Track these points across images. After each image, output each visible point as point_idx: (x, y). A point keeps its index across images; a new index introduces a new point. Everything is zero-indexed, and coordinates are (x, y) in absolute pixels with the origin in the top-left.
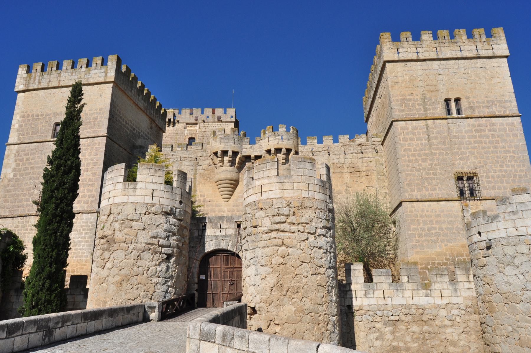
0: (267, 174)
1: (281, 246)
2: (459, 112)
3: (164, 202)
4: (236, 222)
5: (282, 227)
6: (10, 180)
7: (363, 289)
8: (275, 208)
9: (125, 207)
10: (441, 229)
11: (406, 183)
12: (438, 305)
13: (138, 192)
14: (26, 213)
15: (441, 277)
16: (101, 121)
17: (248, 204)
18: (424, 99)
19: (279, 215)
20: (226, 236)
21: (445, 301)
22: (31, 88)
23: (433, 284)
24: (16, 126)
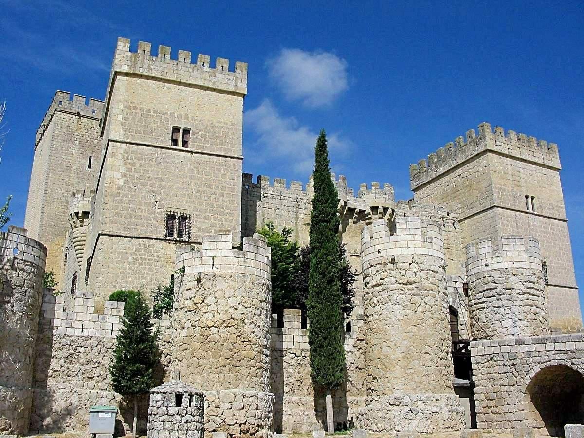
0: (517, 247)
5: (532, 291)
6: (120, 188)
13: (435, 247)
14: (148, 235)
16: (232, 139)
18: (513, 191)
22: (137, 72)
24: (120, 118)
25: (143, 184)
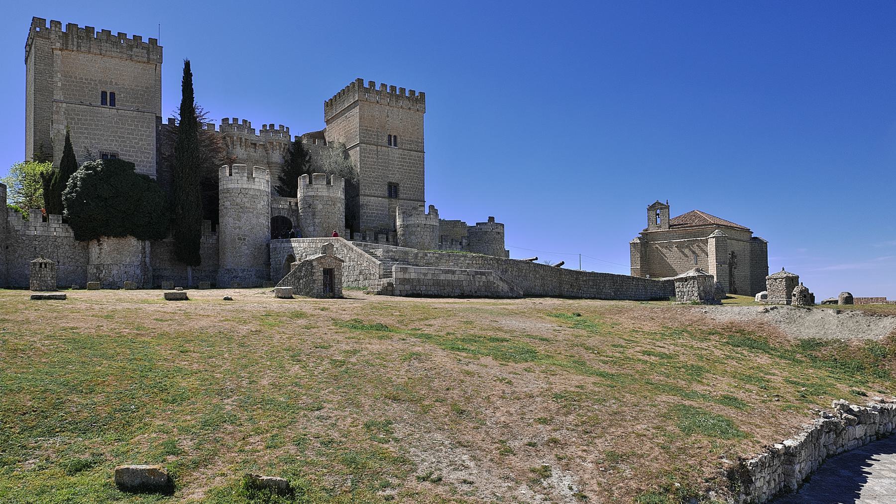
2: (395, 145)
24: (59, 84)
25: (81, 133)
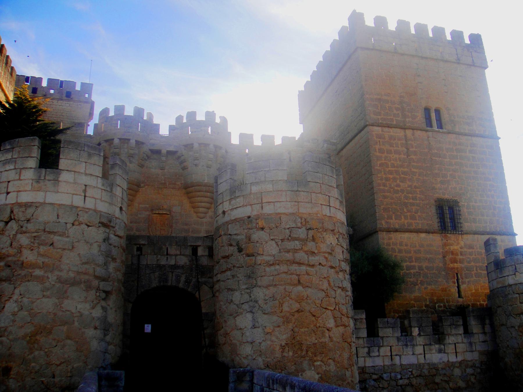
1: (295, 285)
2: (440, 126)
3: (103, 207)
4: (191, 246)
7: (366, 345)
8: (285, 229)
9: (39, 209)
10: (420, 268)
11: (382, 207)
12: (453, 362)
13: (63, 187)
15: (455, 328)
17: (236, 221)
19: (291, 239)
20: (175, 267)
21: (460, 358)
23: (447, 337)
